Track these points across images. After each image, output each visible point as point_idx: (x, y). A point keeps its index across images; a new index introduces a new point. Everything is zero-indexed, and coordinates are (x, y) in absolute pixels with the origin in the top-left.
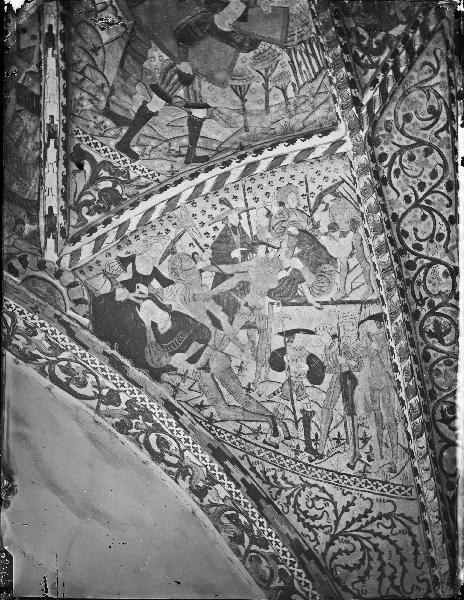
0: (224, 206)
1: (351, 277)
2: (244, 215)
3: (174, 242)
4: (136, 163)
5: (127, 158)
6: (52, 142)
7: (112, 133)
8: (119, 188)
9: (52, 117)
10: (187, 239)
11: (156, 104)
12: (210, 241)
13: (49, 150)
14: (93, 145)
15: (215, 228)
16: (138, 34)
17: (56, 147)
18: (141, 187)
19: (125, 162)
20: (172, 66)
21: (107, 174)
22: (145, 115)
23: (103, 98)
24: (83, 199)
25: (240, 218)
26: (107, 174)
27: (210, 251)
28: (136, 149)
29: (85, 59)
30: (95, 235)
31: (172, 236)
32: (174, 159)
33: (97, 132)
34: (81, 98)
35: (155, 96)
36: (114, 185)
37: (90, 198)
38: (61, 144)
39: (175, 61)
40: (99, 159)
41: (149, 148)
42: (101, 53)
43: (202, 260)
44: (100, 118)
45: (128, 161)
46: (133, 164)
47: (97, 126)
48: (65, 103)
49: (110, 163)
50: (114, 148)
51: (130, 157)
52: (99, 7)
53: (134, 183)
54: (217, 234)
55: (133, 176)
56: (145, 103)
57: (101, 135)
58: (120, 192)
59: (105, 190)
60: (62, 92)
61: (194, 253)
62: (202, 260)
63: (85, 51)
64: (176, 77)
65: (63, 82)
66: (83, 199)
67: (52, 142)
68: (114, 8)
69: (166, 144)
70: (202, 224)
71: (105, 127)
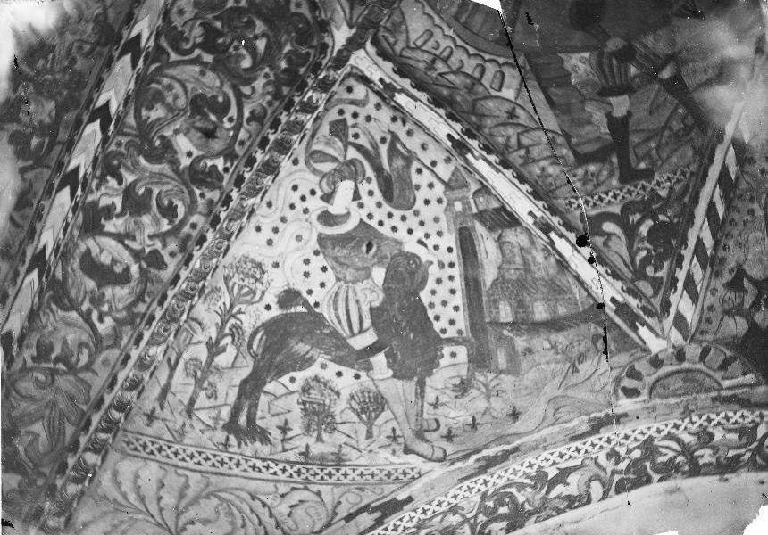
4: (657, 178)
6: (553, 235)
7: (605, 173)
8: (662, 218)
9: (531, 213)
11: (620, 105)
13: (557, 246)
14: (598, 203)
16: (540, 61)
17: (561, 236)
18: (683, 195)
19: (644, 188)
20: (601, 55)
21: (638, 216)
22: (619, 127)
23: (565, 151)
24: (638, 262)
26: (638, 216)
28: (642, 165)
29: (511, 131)
30: (680, 285)
33: (589, 187)
34: (543, 169)
35: (612, 100)
36: (655, 218)
37: (643, 253)
38: (563, 230)
39: (597, 48)
40: (616, 209)
41: (654, 152)
42: (519, 112)
44: (580, 172)
45: (646, 184)
46: (654, 182)
47: (585, 181)
48: (530, 190)
49: (631, 202)
50: (620, 186)
51: (641, 178)
52: (477, 75)
55: (663, 193)
56: (609, 115)
57: (598, 185)
58: (666, 219)
59: (650, 232)
60: (517, 182)
63: (504, 124)
64: (614, 62)
65: (509, 173)
66: (638, 262)
67: (553, 235)
68: (489, 61)
69: (667, 133)
71: (593, 175)
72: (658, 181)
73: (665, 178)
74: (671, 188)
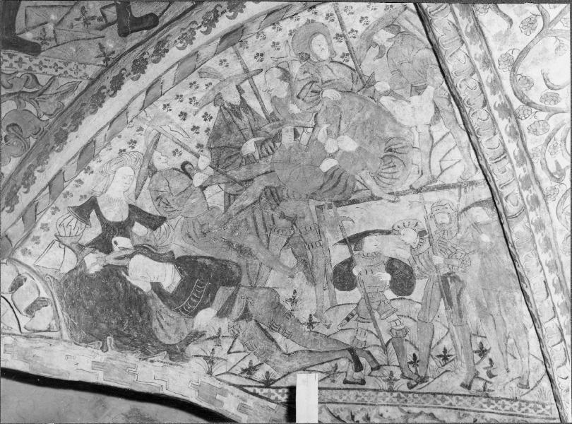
0: (209, 80)
1: (440, 150)
2: (246, 85)
3: (148, 156)
4: (41, 58)
5: (22, 55)
10: (167, 145)
12: (204, 138)
15: (206, 117)
18: (66, 93)
19: (20, 61)
25: (240, 91)
27: (207, 152)
28: (29, 36)
30: (19, 208)
31: (140, 147)
32: (101, 33)
41: (50, 27)
43: (199, 170)
53: (51, 90)
54: (211, 124)
55: (43, 80)
61: (183, 165)
62: (199, 170)
70: (183, 115)
72: (41, 63)
73: (52, 64)
74: (54, 78)
